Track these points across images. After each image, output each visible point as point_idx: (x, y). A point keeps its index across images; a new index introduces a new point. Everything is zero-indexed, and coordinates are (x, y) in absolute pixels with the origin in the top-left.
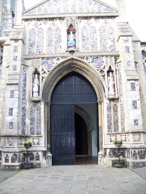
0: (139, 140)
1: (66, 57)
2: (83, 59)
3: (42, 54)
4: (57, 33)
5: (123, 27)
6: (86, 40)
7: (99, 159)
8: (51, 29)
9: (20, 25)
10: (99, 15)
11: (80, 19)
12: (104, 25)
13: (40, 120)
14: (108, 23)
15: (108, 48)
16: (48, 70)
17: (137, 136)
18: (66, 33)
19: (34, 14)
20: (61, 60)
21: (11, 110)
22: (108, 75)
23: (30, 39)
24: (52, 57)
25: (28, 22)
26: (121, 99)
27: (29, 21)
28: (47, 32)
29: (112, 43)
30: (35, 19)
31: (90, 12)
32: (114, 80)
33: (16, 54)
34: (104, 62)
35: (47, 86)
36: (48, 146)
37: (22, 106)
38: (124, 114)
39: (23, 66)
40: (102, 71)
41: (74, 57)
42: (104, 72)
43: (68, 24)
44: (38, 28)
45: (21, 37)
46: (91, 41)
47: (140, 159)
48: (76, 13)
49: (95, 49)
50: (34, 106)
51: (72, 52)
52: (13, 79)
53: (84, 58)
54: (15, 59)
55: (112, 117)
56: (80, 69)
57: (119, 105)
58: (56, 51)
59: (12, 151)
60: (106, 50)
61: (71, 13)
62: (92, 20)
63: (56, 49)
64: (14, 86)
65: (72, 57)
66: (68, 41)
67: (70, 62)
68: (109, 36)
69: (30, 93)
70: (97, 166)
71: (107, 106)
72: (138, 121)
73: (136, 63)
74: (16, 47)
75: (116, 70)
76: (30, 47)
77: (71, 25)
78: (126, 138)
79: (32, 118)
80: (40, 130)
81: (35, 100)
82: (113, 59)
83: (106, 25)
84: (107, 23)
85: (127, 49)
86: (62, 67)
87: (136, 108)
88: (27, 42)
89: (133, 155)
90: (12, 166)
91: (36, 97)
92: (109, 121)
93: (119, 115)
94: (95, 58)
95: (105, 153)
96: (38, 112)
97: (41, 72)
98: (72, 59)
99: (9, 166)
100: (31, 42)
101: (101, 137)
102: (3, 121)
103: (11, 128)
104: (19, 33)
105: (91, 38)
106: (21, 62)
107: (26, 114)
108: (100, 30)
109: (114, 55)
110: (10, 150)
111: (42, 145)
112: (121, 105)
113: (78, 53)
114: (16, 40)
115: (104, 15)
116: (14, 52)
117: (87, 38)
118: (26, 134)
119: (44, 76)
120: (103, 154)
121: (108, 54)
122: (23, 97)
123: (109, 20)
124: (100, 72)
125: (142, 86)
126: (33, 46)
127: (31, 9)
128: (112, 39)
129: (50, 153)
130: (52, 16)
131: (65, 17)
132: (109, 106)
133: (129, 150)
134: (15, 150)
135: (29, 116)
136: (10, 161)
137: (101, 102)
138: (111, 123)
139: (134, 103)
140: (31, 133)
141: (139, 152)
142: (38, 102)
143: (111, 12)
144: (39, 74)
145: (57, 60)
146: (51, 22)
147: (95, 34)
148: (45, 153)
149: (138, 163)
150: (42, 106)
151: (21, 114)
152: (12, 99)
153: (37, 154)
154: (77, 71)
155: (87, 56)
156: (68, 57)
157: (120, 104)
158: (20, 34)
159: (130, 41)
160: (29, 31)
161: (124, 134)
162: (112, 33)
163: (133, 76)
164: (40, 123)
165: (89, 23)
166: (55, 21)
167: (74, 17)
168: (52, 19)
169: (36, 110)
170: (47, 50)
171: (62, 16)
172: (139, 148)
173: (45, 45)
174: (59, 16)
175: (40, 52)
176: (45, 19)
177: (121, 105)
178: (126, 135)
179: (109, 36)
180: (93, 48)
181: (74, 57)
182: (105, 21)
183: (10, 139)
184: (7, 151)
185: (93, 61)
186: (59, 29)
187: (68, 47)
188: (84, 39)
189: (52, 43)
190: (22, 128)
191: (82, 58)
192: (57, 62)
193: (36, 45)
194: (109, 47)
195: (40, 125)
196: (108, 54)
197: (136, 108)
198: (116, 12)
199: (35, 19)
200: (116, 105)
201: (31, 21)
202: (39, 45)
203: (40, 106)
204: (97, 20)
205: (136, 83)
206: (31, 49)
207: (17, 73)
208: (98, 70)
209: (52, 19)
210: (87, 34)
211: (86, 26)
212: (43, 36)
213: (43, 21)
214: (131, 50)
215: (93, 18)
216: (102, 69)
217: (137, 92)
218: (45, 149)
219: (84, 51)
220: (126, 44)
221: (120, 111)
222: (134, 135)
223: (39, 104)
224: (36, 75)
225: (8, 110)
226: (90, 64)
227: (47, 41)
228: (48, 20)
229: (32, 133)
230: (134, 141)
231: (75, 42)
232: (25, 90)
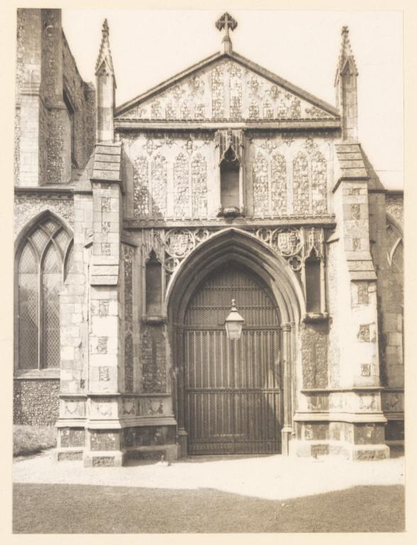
1: (216, 229)
8: (185, 158)
14: (315, 145)
20: (208, 237)
28: (176, 165)
42: (299, 262)
44: (155, 153)
65: (231, 228)
84: (311, 145)
85: (355, 208)
98: (232, 233)
128: (321, 187)
156: (224, 227)
194: (313, 207)
227: (176, 190)
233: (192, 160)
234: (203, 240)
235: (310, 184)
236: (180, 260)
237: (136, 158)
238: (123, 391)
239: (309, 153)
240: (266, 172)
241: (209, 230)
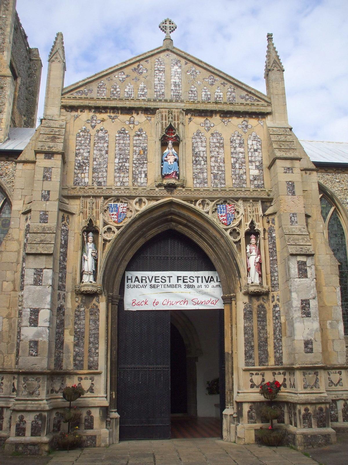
0: (316, 385)
2: (195, 205)
3: (104, 188)
4: (138, 142)
5: (283, 138)
6: (203, 162)
7: (225, 426)
8: (127, 132)
9: (56, 118)
10: (230, 108)
11: (189, 116)
12: (241, 132)
13: (96, 337)
14: (250, 126)
15: (248, 182)
16: (116, 225)
17: (311, 376)
18: (158, 144)
19: (89, 96)
20: (148, 205)
21: (35, 312)
22: (248, 242)
23: (77, 152)
24: (126, 196)
25: (74, 113)
26: (275, 295)
27: (77, 111)
29: (256, 172)
30: (89, 108)
31: (212, 100)
32: (259, 253)
33: (48, 186)
34: (240, 213)
36: (111, 395)
37: (58, 304)
38: (281, 326)
39: (61, 214)
40: (234, 232)
41: (174, 199)
42: (238, 234)
43: (162, 125)
44: (98, 127)
45: (59, 147)
46: (213, 164)
47: (319, 426)
48: (182, 102)
49: (221, 184)
50: (85, 304)
51: (171, 187)
52: (42, 242)
53: (196, 201)
54: (46, 197)
55: (255, 331)
56: (185, 225)
57: (269, 306)
58: (136, 184)
59: (34, 409)
60: (244, 185)
61: (171, 101)
62: (216, 119)
63: (135, 179)
64: (44, 258)
65: (171, 198)
66: (162, 162)
67: (166, 209)
68: (252, 156)
69: (76, 274)
70: (220, 442)
71: (245, 309)
72: (312, 343)
73: (307, 216)
74: (47, 170)
75: (264, 230)
76: (78, 171)
77: (170, 129)
78: (285, 379)
79: (79, 331)
80: (96, 358)
81: (86, 291)
82: (259, 206)
83: (246, 131)
84: (247, 126)
85: (291, 186)
87: (308, 315)
88: (71, 158)
89: (304, 418)
90: (34, 444)
91: (90, 283)
92: (248, 343)
93: (270, 329)
94: (220, 203)
95: (240, 413)
96: (93, 317)
97: (102, 229)
98: (171, 203)
99: (26, 445)
100: (80, 158)
101: (230, 376)
102: (10, 337)
103: (34, 353)
104: (54, 139)
105: (213, 159)
106: (59, 205)
107: (66, 323)
108: (231, 142)
109: (262, 199)
110: (30, 405)
111: (100, 393)
112: (275, 306)
113: (184, 190)
114: (49, 154)
115: (242, 109)
116: (43, 181)
117: (205, 158)
118: (64, 367)
119: (108, 239)
120: (235, 415)
121: (248, 195)
122: (60, 283)
123: (253, 122)
124: (231, 233)
125: (320, 268)
126: (84, 168)
127: (80, 84)
128: (258, 164)
129: (115, 412)
130: (128, 104)
131: (158, 109)
132: (249, 309)
133: (295, 408)
134: (42, 406)
135: (71, 326)
136: (28, 432)
138: (252, 347)
139: (305, 304)
140: (75, 365)
141: (315, 411)
143: (256, 103)
144: (96, 232)
145: (138, 204)
146: (126, 118)
147: (221, 151)
148: (105, 411)
149: (314, 436)
150: (102, 305)
151: (56, 321)
152: (38, 288)
153: (89, 413)
154: (180, 228)
155: (203, 198)
157: (272, 305)
158: (57, 140)
159: (297, 171)
160: (75, 133)
161: (281, 372)
162: (259, 151)
163: (301, 246)
164: (95, 344)
165: (208, 125)
166: (135, 115)
167: (176, 110)
169: (88, 314)
170: (117, 180)
171: (152, 105)
172: (314, 402)
173: (111, 168)
174: (143, 105)
175: (99, 183)
176: (114, 109)
177: (275, 306)
178: (284, 374)
179: (252, 156)
180: (216, 181)
181: (174, 199)
182: (244, 122)
183: (31, 380)
184: (22, 408)
185: (216, 209)
186: (144, 135)
187: (164, 177)
188: (197, 159)
189: (127, 164)
190: (56, 354)
191: (191, 202)
192: (137, 207)
193: (91, 166)
194: (251, 181)
195: (97, 348)
196: (247, 196)
197: (308, 315)
198: (266, 104)
199: (89, 108)
200: (263, 307)
201: (81, 111)
202: (98, 167)
203: (97, 304)
204: (225, 119)
205: (309, 262)
206: (79, 175)
207: (49, 228)
208: (226, 230)
210: (204, 149)
211: (202, 129)
212: (108, 147)
213: (108, 114)
214: (298, 190)
215: (218, 116)
216: (236, 228)
217: (309, 281)
218: (106, 403)
219: (198, 185)
220: (289, 177)
221: (271, 319)
222: (304, 374)
223: (94, 301)
224: (91, 234)
225: (29, 313)
226: (210, 216)
227: (117, 160)
228: (120, 112)
229: (79, 365)
230: (305, 388)
231: (178, 165)
232: (65, 268)
233: (134, 134)
234: (144, 207)
235: (247, 160)
236: (118, 228)
237: (80, 131)
238: (52, 367)
239: (245, 133)
240: (205, 147)
241: (148, 200)
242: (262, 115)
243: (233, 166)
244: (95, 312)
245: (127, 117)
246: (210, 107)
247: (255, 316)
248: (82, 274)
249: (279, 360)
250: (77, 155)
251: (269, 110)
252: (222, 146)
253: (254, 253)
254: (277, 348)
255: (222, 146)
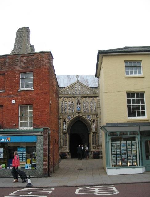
22: (93, 123)
30: (63, 97)
35: (69, 127)
50: (64, 135)
51: (79, 113)
57: (97, 134)
62: (87, 98)
63: (72, 111)
77: (79, 101)
86: (75, 119)
92: (93, 141)
93: (97, 139)
95: (91, 153)
97: (67, 121)
98: (79, 116)
123: (95, 98)
130: (70, 96)
137: (90, 133)
142: (66, 133)
144: (65, 122)
150: (67, 135)
154: (80, 120)
164: (66, 142)
168: (70, 97)
171: (75, 96)
173: (68, 109)
175: (66, 112)
176: (68, 97)
187: (77, 111)
191: (82, 115)
199: (63, 97)
209: (70, 97)
211: (85, 101)
229: (64, 145)
234: (74, 117)
242: (96, 97)
243: (91, 108)
244: (66, 136)
245: (70, 98)
246: (86, 96)
247: (94, 137)
248: (63, 129)
249: (98, 144)
250: (61, 107)
251: (98, 95)
252: (88, 104)
253: (94, 125)
254: (98, 142)
255: (88, 104)
